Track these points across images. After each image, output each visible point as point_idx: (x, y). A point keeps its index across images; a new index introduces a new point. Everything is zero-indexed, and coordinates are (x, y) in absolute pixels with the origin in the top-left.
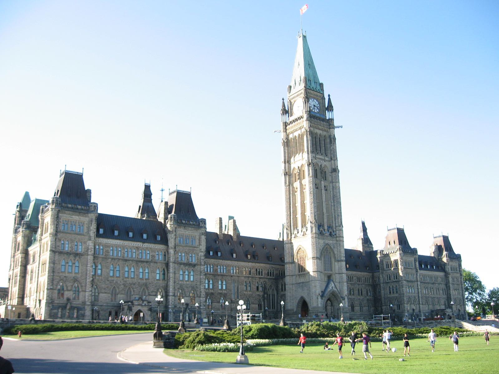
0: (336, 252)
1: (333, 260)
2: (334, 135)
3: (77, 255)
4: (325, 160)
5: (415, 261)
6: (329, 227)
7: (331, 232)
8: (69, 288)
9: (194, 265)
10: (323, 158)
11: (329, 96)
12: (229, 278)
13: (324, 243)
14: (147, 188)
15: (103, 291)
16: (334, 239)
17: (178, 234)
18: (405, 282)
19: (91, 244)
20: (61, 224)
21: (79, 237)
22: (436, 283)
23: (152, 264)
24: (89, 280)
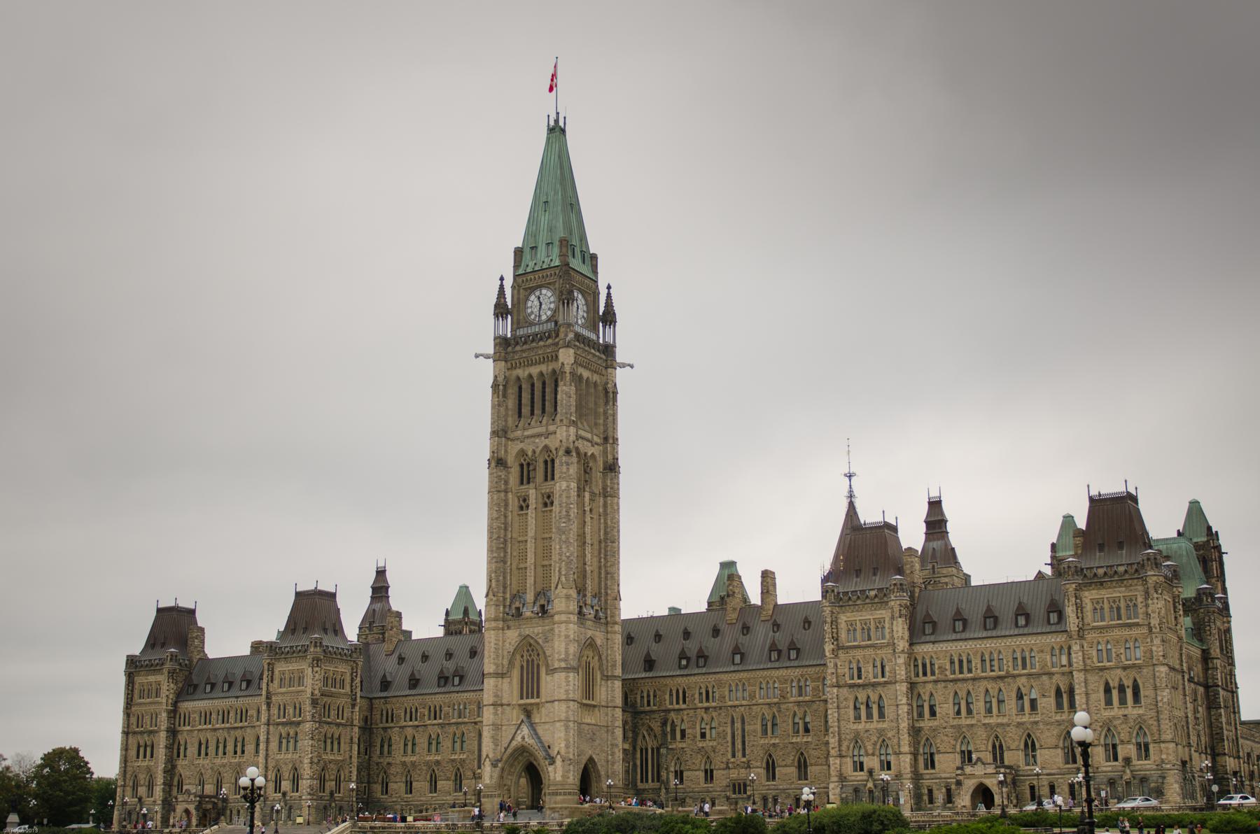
0: (548, 653)
1: (543, 671)
3: (151, 732)
4: (548, 435)
5: (893, 618)
6: (537, 595)
7: (542, 607)
9: (299, 723)
10: (542, 430)
12: (471, 727)
13: (520, 635)
14: (381, 573)
17: (276, 672)
18: (835, 690)
19: (164, 715)
20: (136, 692)
21: (153, 707)
22: (1014, 676)
23: (248, 730)
24: (161, 766)
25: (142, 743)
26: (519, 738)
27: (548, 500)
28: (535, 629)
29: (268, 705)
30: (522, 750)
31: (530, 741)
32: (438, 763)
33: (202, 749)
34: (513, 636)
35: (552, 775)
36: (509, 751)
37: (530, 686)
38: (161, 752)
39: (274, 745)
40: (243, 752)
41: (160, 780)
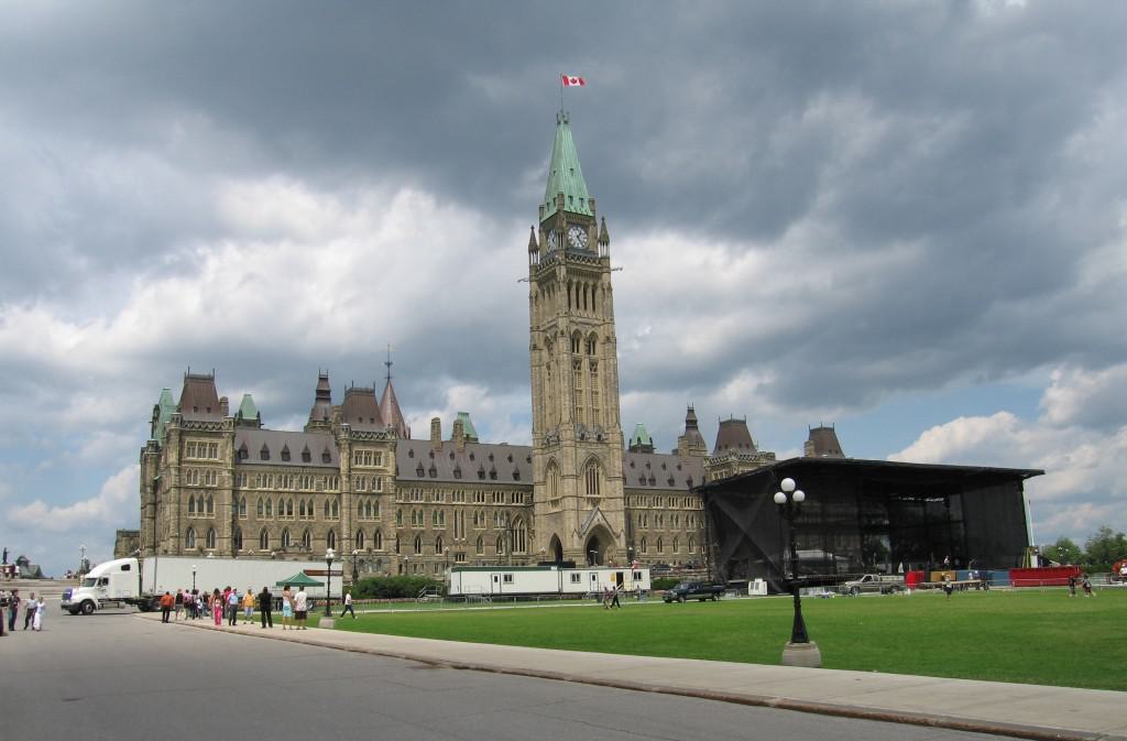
1: (602, 479)
2: (609, 284)
3: (210, 489)
8: (201, 534)
9: (380, 494)
11: (603, 219)
15: (249, 535)
16: (604, 447)
24: (228, 521)
25: (196, 498)
26: (596, 520)
27: (593, 365)
28: (599, 450)
29: (349, 477)
30: (599, 528)
31: (603, 522)
32: (423, 532)
33: (263, 505)
34: (582, 454)
35: (618, 544)
36: (591, 528)
37: (593, 485)
38: (228, 511)
39: (355, 511)
40: (311, 512)
41: (227, 532)
